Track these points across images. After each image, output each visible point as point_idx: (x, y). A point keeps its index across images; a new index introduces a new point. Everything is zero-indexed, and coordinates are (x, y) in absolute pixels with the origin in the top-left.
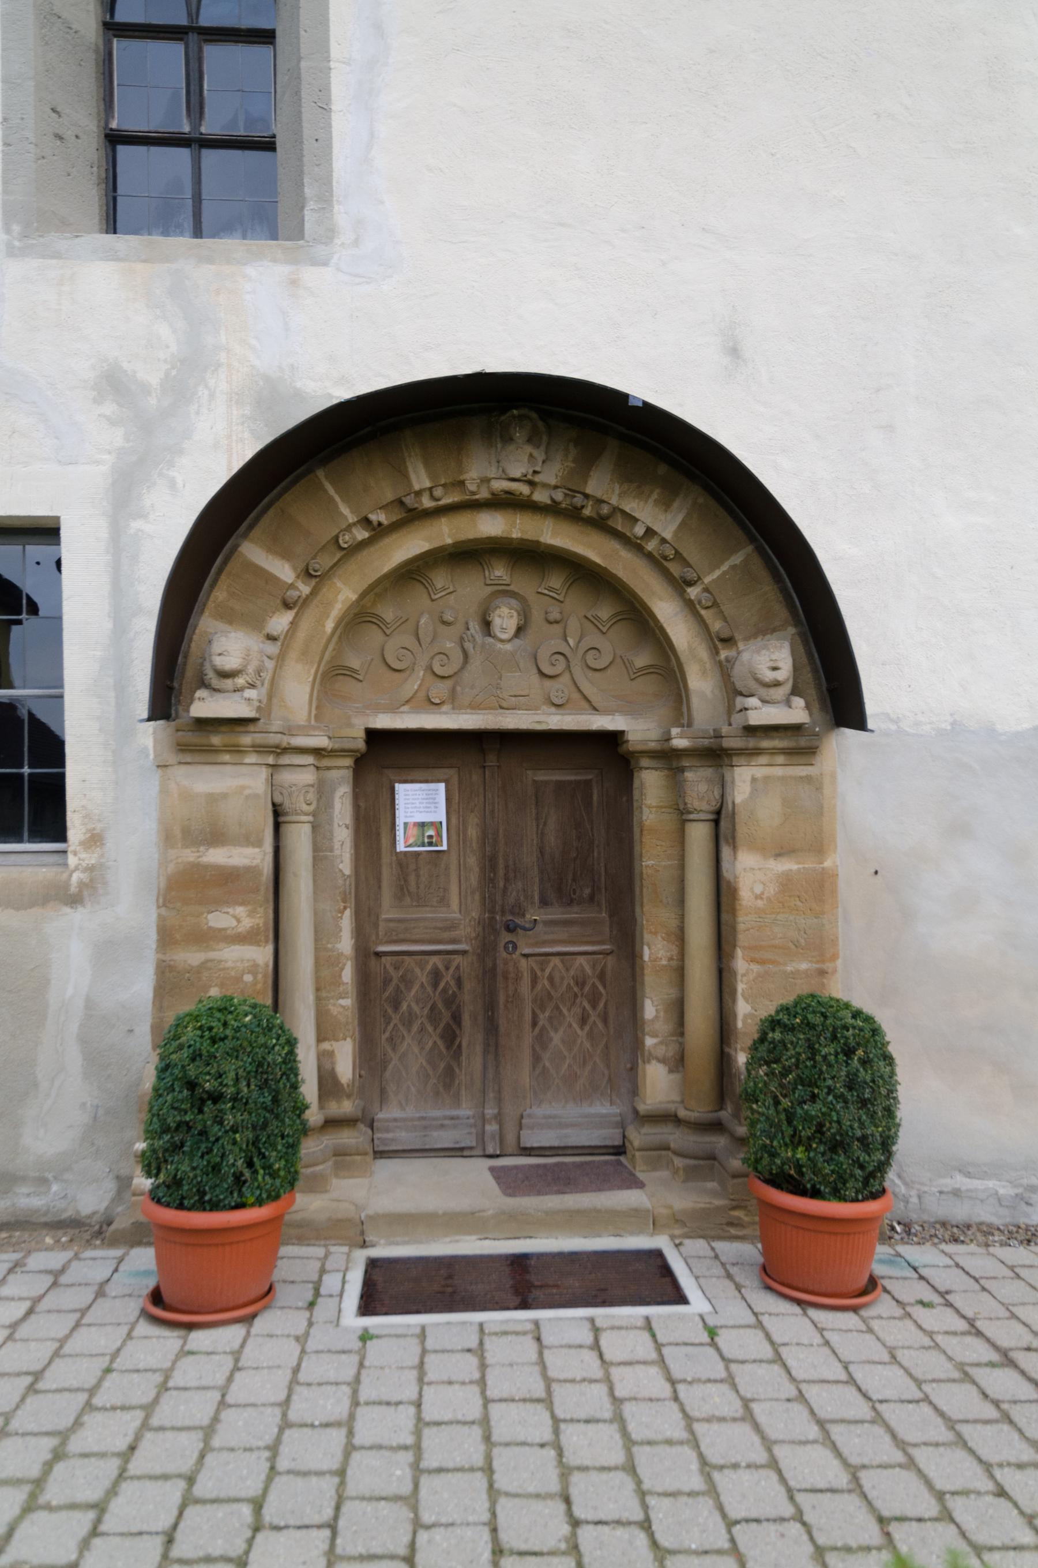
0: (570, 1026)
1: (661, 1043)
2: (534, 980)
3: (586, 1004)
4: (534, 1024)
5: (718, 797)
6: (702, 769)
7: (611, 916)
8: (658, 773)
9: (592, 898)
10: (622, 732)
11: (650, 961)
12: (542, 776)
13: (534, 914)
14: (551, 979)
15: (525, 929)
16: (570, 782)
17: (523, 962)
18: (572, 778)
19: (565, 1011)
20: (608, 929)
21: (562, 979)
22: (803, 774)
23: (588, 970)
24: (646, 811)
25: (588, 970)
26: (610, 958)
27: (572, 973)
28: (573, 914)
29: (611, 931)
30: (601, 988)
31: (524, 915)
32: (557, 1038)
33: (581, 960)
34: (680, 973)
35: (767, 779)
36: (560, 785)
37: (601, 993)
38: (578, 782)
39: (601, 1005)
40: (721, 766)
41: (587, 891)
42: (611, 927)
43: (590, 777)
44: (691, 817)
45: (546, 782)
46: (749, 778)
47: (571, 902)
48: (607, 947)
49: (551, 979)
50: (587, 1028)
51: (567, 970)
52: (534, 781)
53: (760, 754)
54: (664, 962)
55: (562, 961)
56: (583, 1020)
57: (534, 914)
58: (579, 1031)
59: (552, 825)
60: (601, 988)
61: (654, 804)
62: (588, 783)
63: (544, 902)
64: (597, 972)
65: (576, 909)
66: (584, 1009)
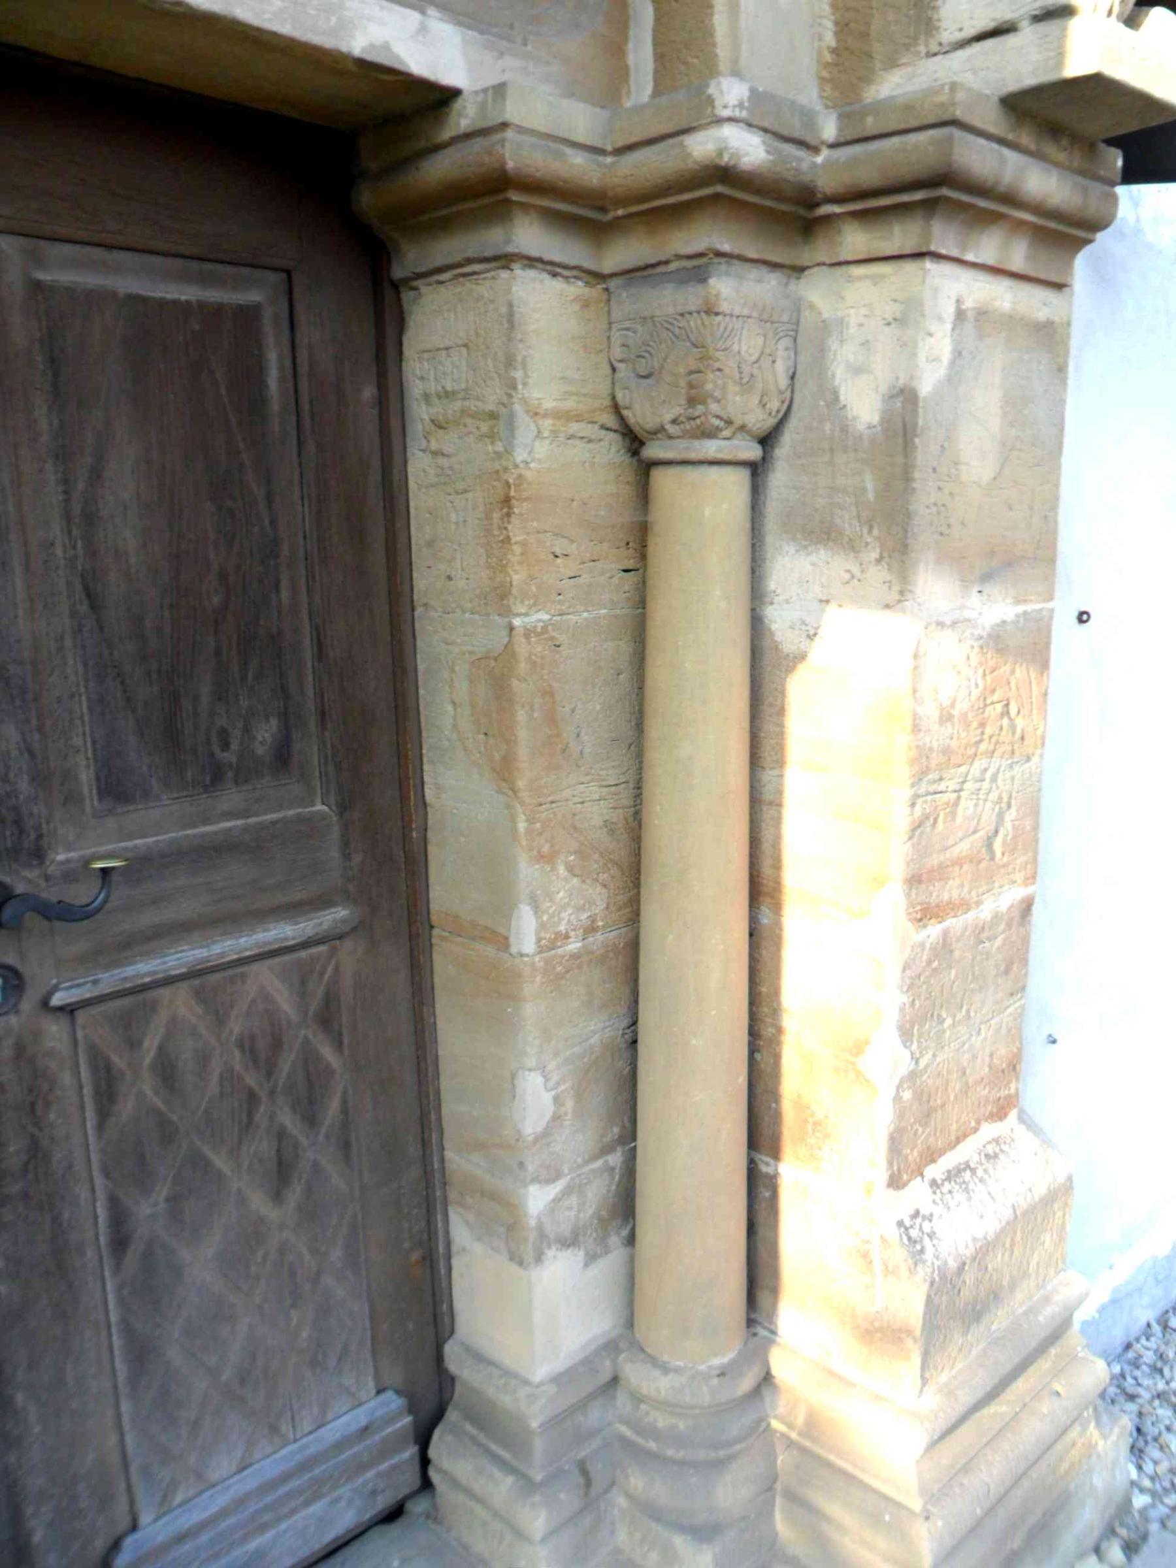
0: (242, 1201)
1: (567, 1192)
2: (107, 1092)
3: (288, 1119)
4: (120, 1243)
5: (783, 382)
6: (755, 272)
7: (343, 808)
8: (558, 285)
9: (282, 757)
10: (448, 95)
11: (541, 950)
12: (67, 270)
13: (88, 844)
14: (166, 1071)
15: (62, 914)
16: (185, 309)
17: (55, 1032)
18: (188, 293)
19: (220, 1161)
20: (335, 854)
21: (203, 1059)
22: (1042, 315)
23: (285, 1002)
24: (525, 428)
25: (285, 1002)
26: (348, 944)
27: (236, 1026)
28: (228, 816)
29: (346, 856)
30: (327, 1053)
31: (38, 855)
32: (200, 1265)
33: (265, 977)
34: (627, 963)
35: (983, 314)
36: (148, 321)
37: (329, 1071)
38: (214, 314)
39: (332, 1109)
40: (801, 270)
41: (266, 733)
42: (345, 843)
43: (253, 296)
44: (712, 448)
45: (95, 299)
46: (949, 310)
47: (216, 776)
48: (337, 915)
49: (166, 1071)
50: (295, 1194)
51: (220, 1019)
52: (37, 288)
53: (993, 218)
54: (574, 946)
55: (198, 994)
56: (282, 1172)
57: (88, 844)
58: (272, 1214)
59: (124, 482)
60: (327, 1053)
61: (548, 404)
62: (246, 319)
63: (116, 789)
64: (314, 1006)
65: (231, 797)
66: (282, 1135)
